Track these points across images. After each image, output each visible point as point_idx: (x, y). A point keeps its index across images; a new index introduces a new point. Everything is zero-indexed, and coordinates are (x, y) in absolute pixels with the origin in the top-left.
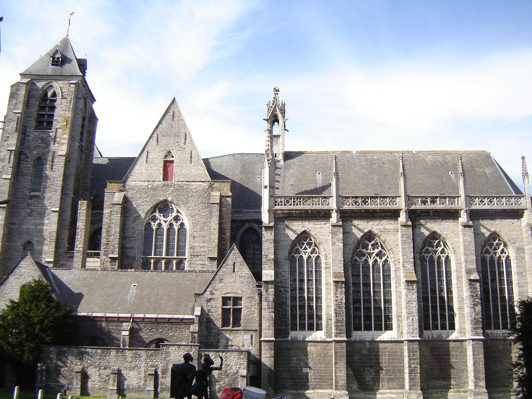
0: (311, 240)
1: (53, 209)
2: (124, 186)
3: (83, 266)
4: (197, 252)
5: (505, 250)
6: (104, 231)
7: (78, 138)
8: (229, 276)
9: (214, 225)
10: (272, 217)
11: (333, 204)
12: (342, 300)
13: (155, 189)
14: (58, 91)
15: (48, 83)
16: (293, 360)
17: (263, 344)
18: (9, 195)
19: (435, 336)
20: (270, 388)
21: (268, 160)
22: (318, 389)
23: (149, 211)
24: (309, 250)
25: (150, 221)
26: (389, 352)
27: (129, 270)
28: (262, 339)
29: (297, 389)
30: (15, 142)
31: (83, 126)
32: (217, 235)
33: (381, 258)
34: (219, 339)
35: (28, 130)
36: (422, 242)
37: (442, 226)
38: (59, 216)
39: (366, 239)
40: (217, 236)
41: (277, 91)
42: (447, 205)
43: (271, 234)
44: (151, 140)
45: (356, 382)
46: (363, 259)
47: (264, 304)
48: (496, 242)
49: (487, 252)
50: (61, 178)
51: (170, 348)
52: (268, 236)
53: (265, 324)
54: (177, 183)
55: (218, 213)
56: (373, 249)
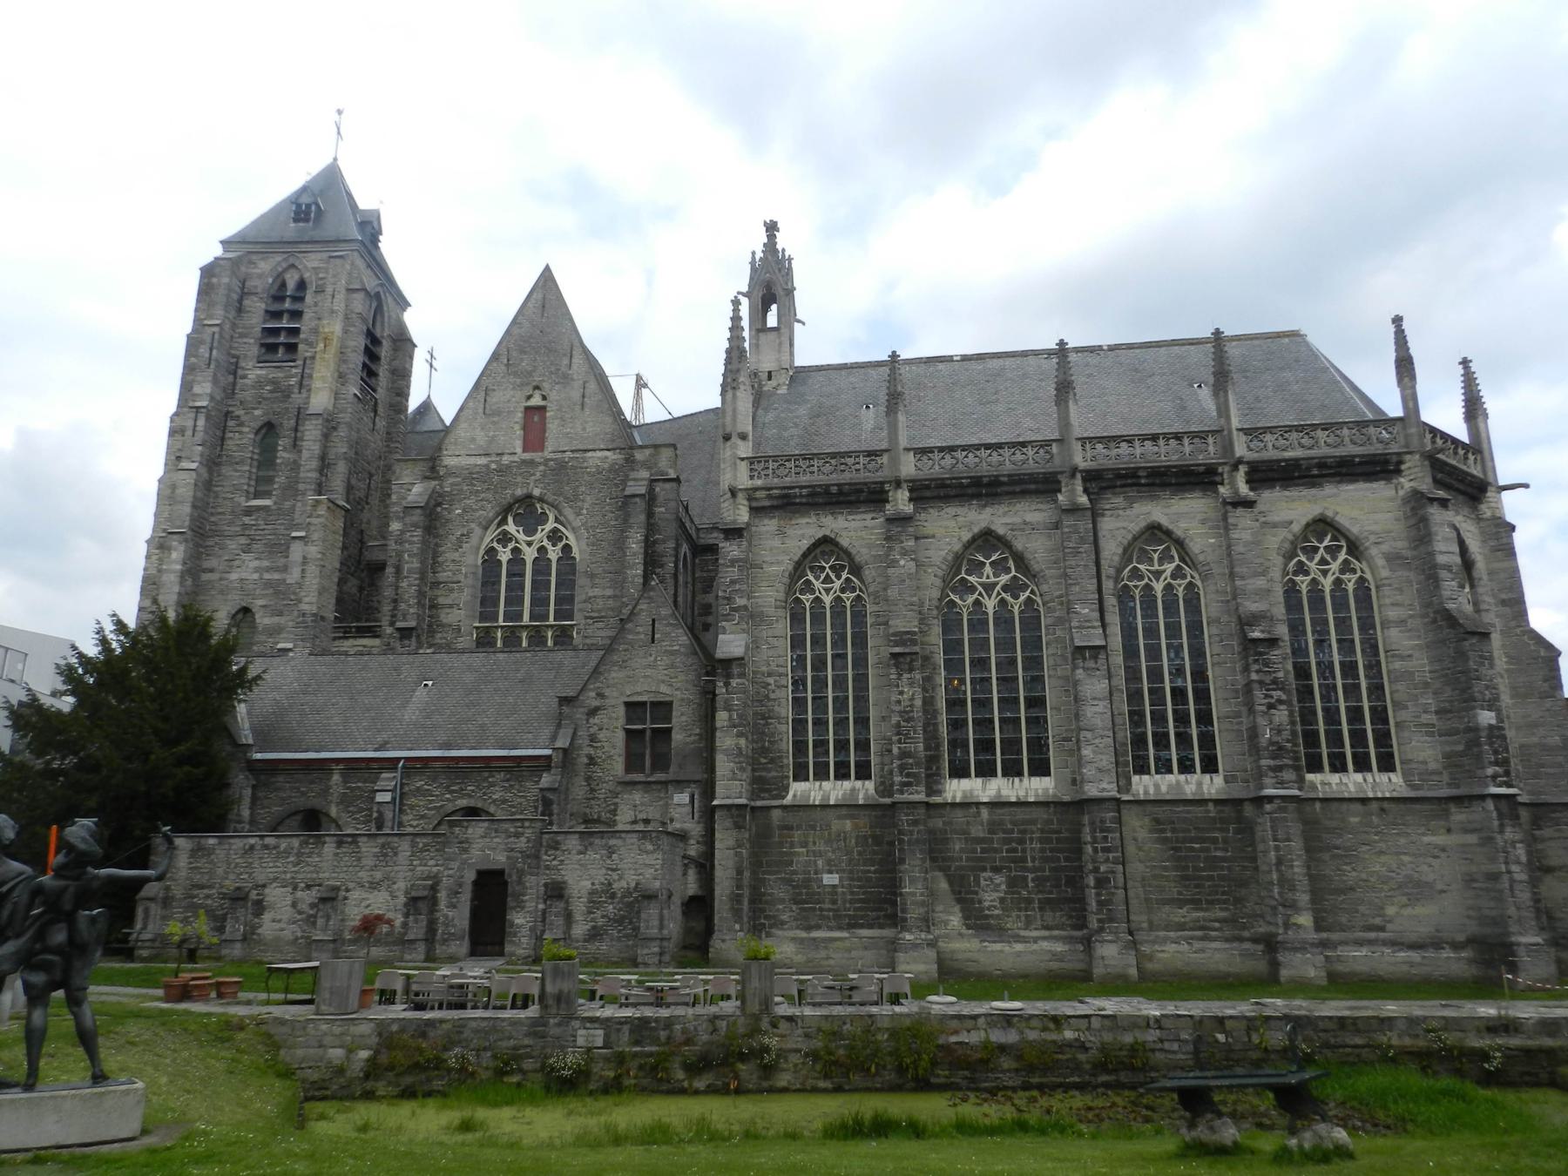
5: (1356, 564)
12: (912, 699)
13: (502, 470)
16: (798, 854)
19: (1164, 789)
20: (737, 927)
22: (862, 926)
24: (837, 584)
25: (495, 544)
26: (1042, 831)
29: (809, 928)
33: (1016, 597)
34: (616, 804)
36: (1120, 551)
37: (1174, 509)
39: (979, 549)
41: (771, 228)
45: (957, 909)
46: (971, 599)
48: (1326, 543)
49: (1302, 569)
51: (470, 831)
53: (723, 765)
55: (642, 517)
56: (995, 575)
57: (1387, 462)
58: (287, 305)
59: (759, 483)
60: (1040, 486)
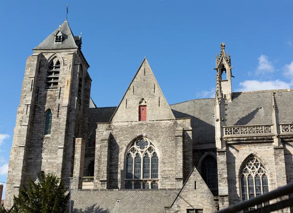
0: (258, 161)
1: (59, 147)
2: (110, 126)
3: (80, 187)
4: (167, 175)
6: (96, 161)
7: (76, 93)
8: (192, 193)
9: (180, 153)
10: (225, 144)
11: (274, 130)
13: (132, 127)
14: (61, 60)
15: (54, 55)
18: (27, 138)
21: (218, 99)
23: (129, 145)
24: (257, 170)
25: (130, 152)
27: (114, 190)
30: (31, 99)
31: (80, 85)
32: (182, 161)
35: (40, 89)
38: (64, 151)
40: (182, 161)
43: (224, 157)
44: (129, 91)
50: (65, 123)
52: (221, 159)
54: (149, 122)
55: (182, 143)
58: (54, 70)
59: (229, 136)
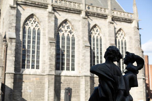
5: (124, 37)
10: (15, 3)
17: (6, 75)
28: (6, 72)
42: (102, 12)
47: (9, 52)
57: (131, 21)
60: (78, 13)
